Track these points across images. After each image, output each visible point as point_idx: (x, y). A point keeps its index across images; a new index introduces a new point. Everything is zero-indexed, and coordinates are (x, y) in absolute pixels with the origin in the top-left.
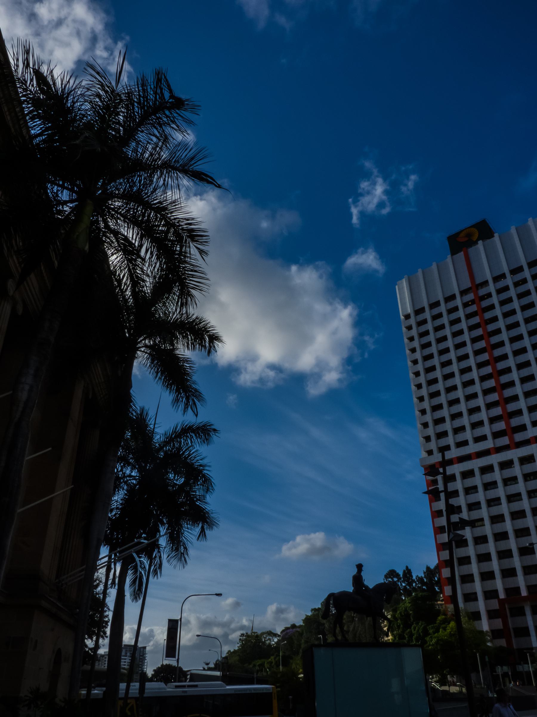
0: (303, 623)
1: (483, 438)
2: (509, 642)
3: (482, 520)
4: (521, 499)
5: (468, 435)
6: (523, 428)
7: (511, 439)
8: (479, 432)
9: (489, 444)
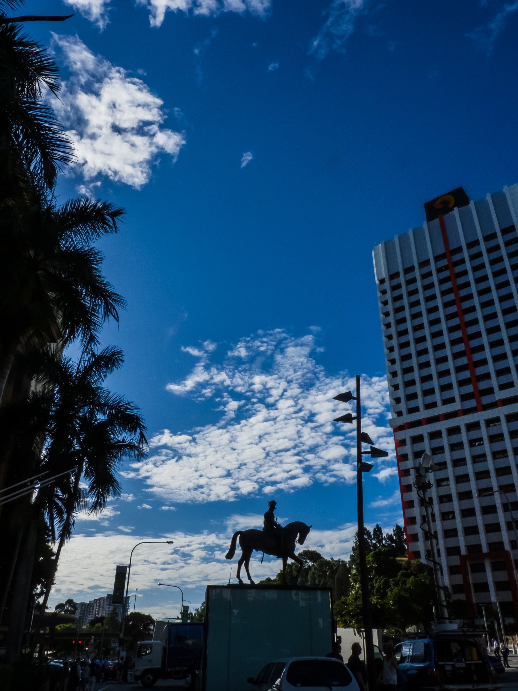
1: (452, 400)
2: (469, 597)
4: (486, 461)
5: (437, 397)
6: (490, 391)
7: (479, 402)
9: (457, 406)
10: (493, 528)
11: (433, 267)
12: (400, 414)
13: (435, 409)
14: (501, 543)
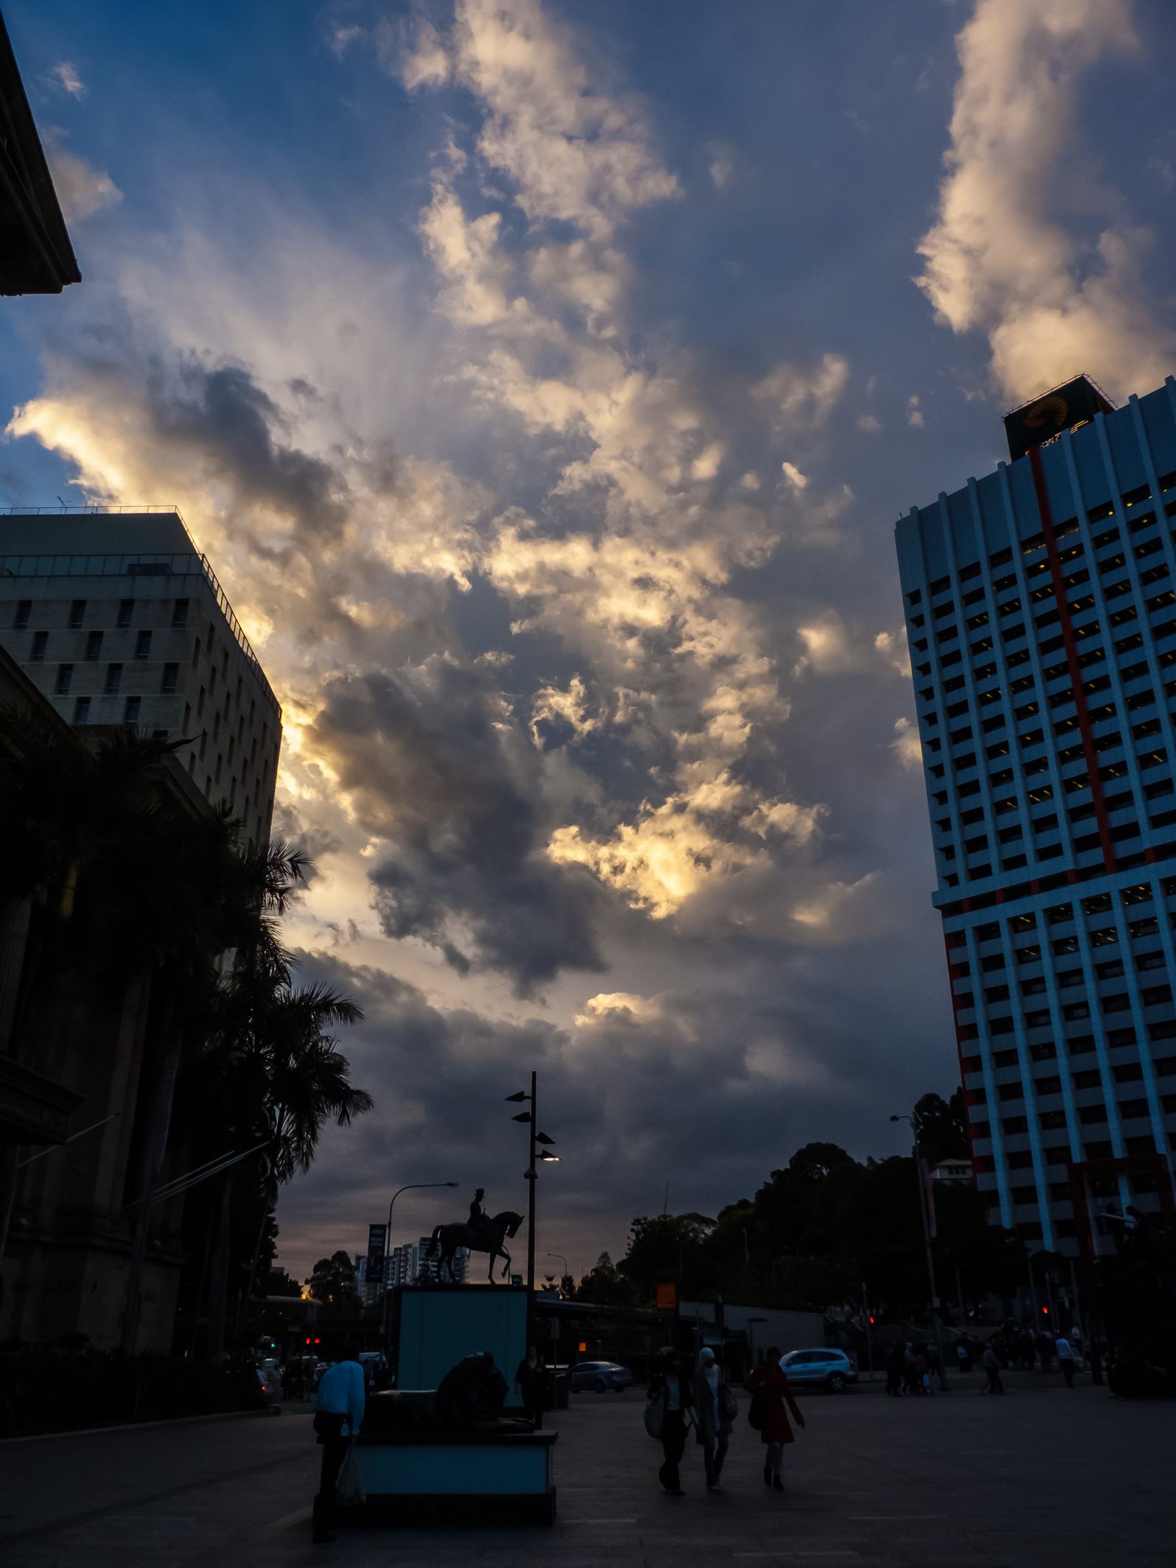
0: (756, 1198)
3: (1046, 1012)
4: (1122, 974)
5: (1027, 845)
6: (1132, 830)
7: (1108, 853)
8: (1047, 839)
9: (1065, 863)
10: (1134, 1109)
11: (1017, 566)
12: (952, 880)
13: (1023, 869)
14: (1150, 1139)
